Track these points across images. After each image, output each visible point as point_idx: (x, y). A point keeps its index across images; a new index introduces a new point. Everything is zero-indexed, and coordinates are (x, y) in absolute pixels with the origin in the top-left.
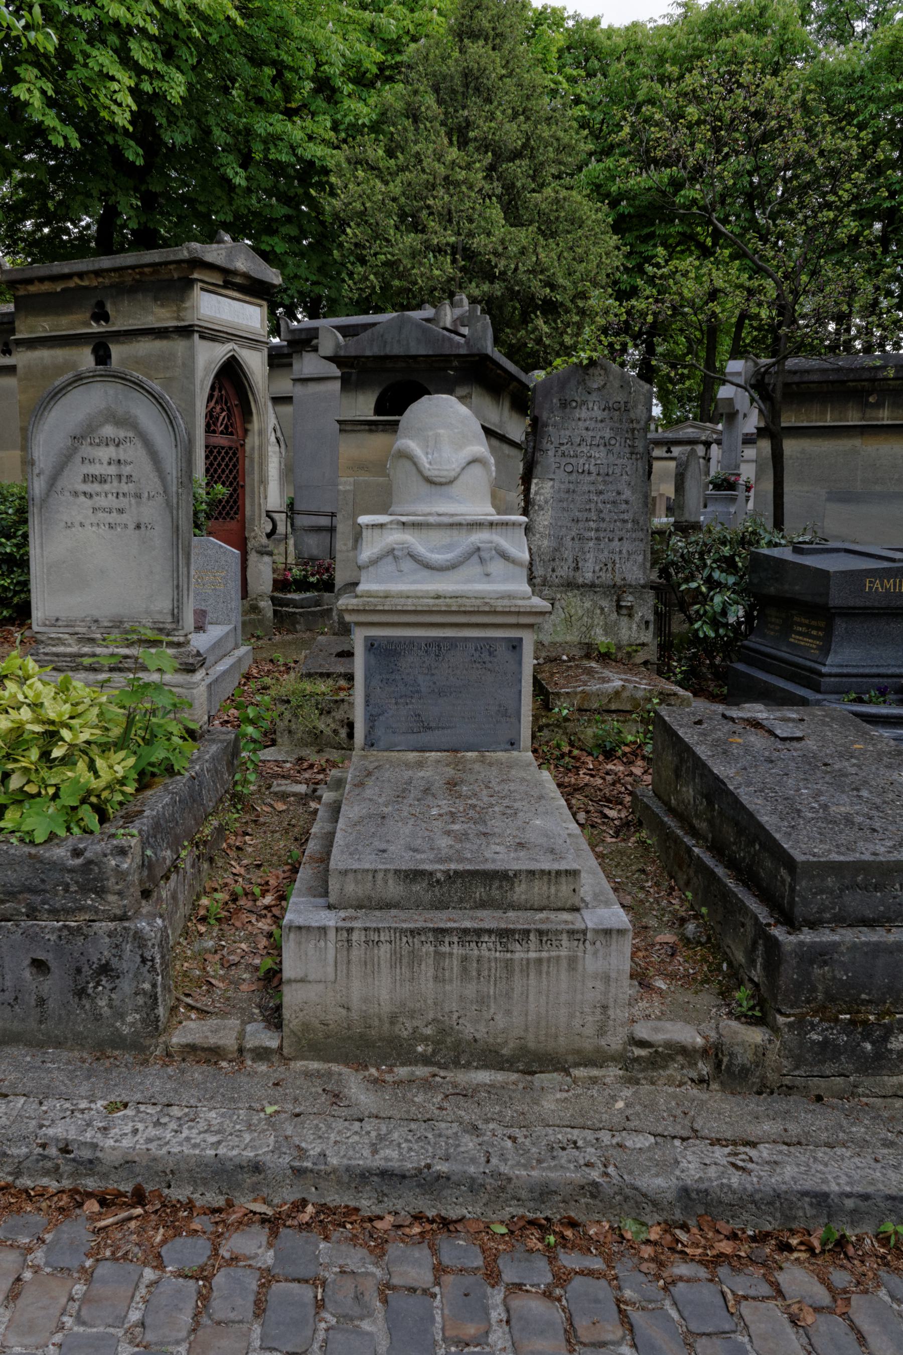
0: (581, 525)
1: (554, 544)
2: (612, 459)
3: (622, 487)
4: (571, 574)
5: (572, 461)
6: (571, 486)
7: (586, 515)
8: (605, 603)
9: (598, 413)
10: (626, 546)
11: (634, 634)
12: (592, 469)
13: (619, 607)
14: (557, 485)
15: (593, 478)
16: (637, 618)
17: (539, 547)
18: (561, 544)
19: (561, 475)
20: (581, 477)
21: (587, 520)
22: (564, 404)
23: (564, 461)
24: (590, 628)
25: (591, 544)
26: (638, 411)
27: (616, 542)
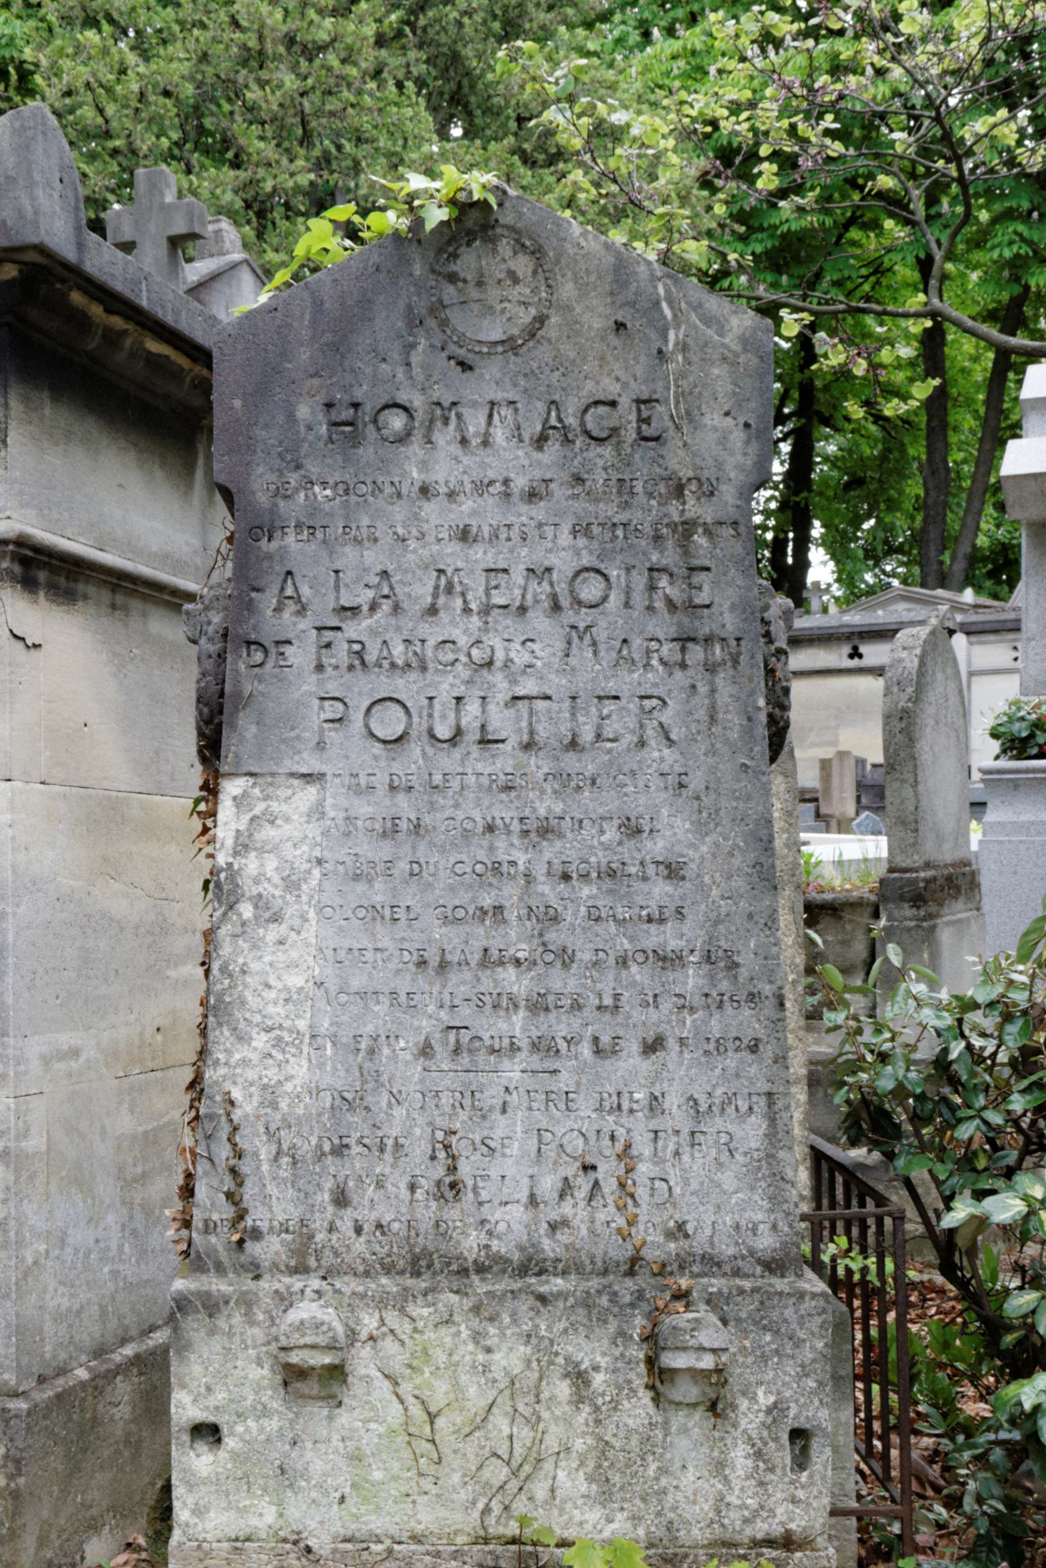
0: (460, 984)
1: (339, 1078)
2: (590, 670)
3: (648, 799)
4: (427, 1212)
5: (403, 686)
6: (405, 807)
7: (480, 935)
8: (592, 1351)
9: (513, 460)
10: (682, 1076)
11: (742, 1495)
12: (502, 721)
13: (659, 1376)
14: (335, 799)
15: (504, 761)
16: (750, 1415)
17: (270, 1095)
18: (370, 1078)
19: (351, 753)
20: (448, 761)
21: (488, 961)
22: (349, 424)
23: (362, 689)
24: (525, 1468)
25: (512, 1071)
26: (706, 441)
27: (630, 1060)
